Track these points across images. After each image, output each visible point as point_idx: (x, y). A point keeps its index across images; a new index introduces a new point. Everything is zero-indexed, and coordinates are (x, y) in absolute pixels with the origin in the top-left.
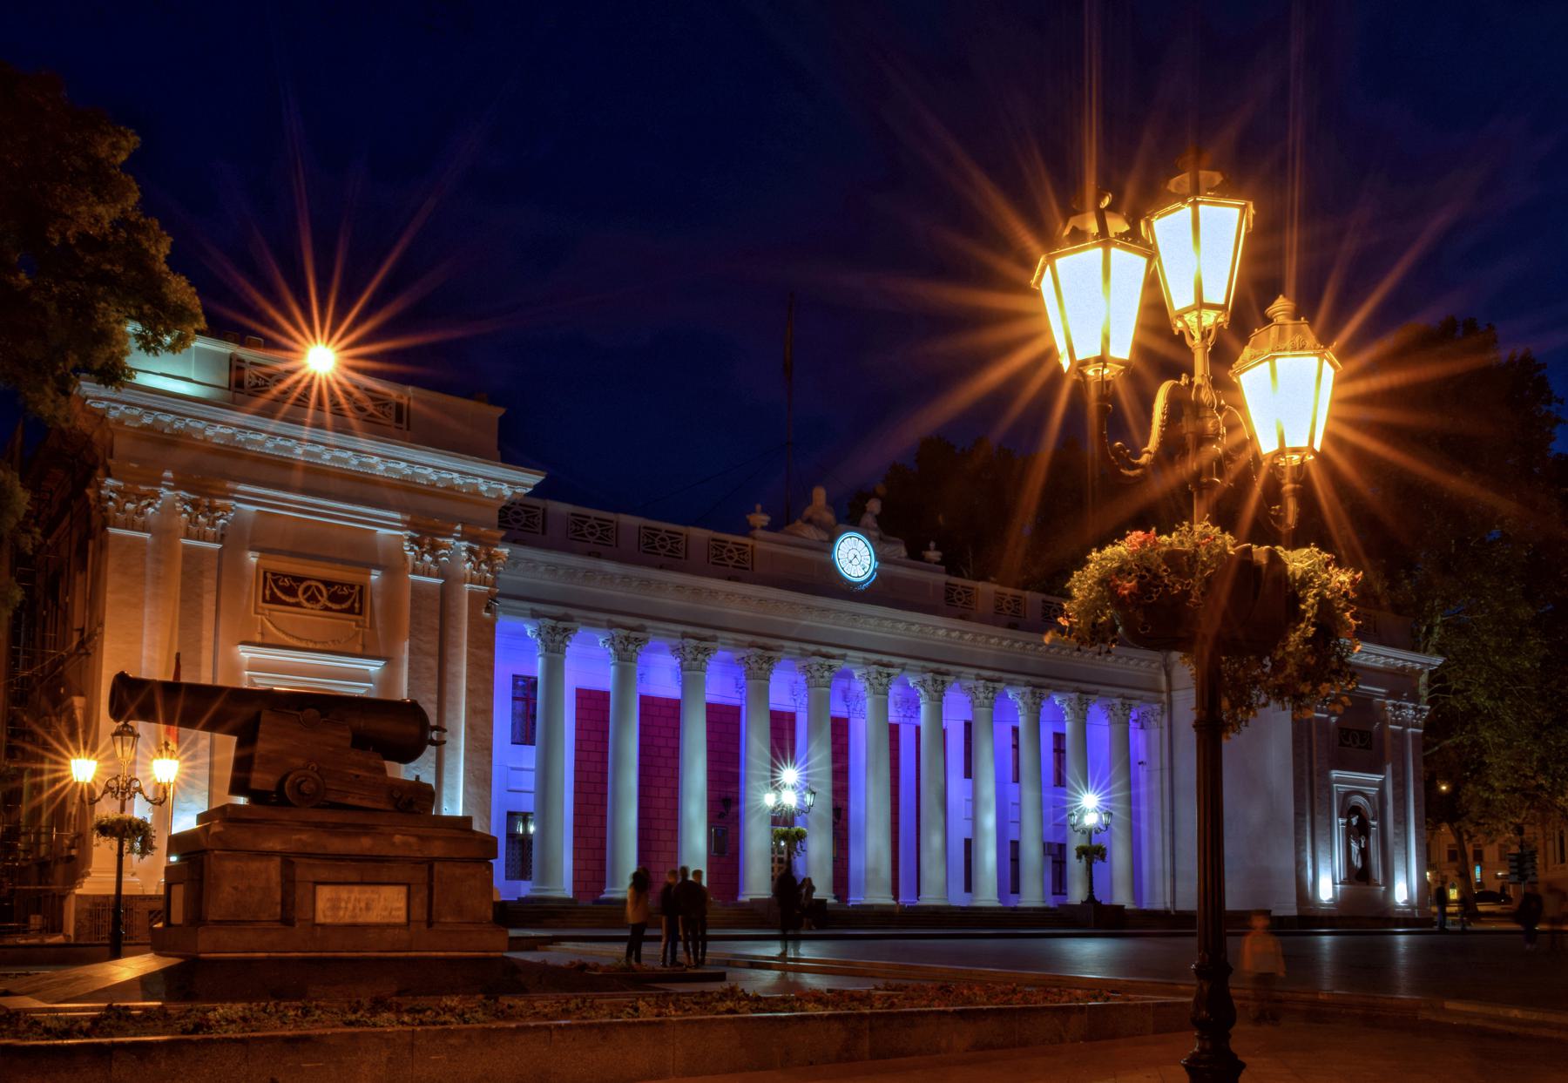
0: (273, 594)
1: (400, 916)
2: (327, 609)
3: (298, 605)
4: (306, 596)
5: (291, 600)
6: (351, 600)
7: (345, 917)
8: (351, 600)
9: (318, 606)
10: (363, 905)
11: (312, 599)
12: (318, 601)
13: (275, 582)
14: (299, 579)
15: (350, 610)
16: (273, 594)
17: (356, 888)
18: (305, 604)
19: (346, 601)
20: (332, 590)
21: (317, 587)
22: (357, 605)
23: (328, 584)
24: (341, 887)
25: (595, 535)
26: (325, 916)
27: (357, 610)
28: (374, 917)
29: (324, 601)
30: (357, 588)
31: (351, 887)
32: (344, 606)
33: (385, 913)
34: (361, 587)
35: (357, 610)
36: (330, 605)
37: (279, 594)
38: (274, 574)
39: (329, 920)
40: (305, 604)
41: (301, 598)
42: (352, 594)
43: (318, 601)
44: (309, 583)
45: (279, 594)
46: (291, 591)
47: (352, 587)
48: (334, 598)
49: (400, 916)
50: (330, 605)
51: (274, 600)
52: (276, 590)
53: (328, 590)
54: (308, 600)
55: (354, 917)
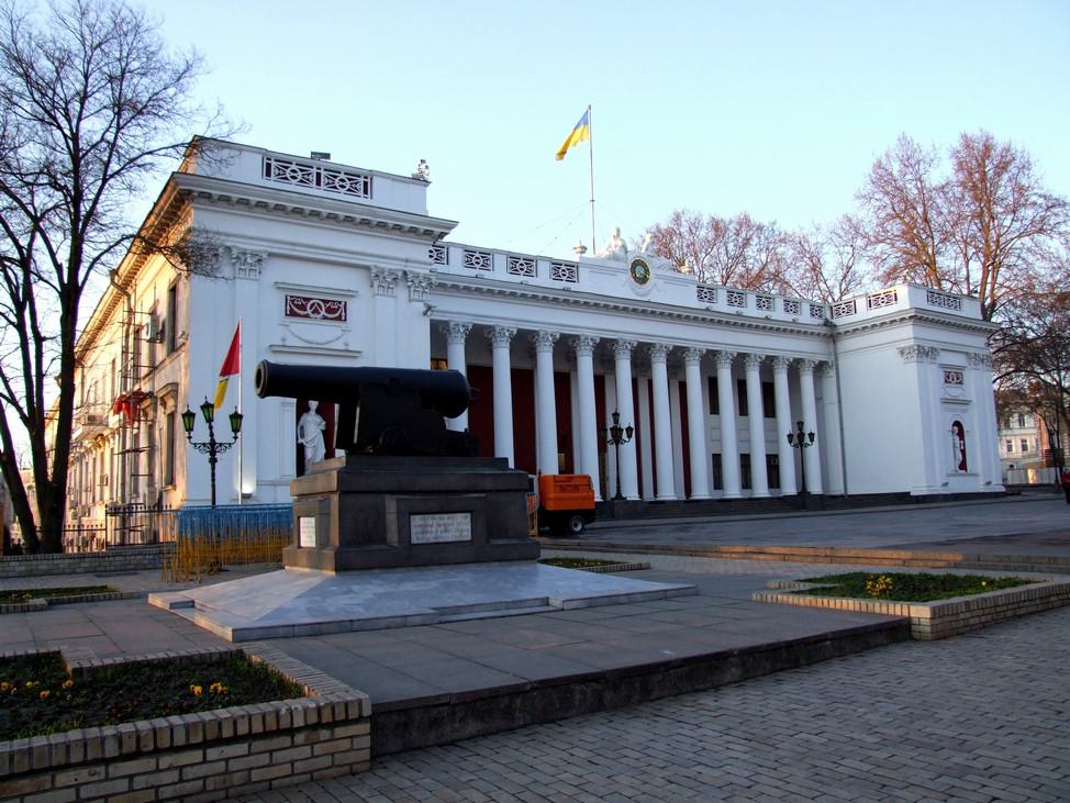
0: (291, 310)
1: (467, 536)
2: (325, 318)
3: (307, 316)
5: (302, 312)
7: (431, 538)
10: (443, 528)
11: (316, 311)
13: (293, 302)
14: (308, 300)
16: (291, 310)
17: (437, 516)
18: (312, 315)
23: (325, 301)
24: (427, 516)
26: (418, 539)
28: (450, 537)
29: (323, 313)
32: (337, 315)
33: (457, 534)
39: (420, 542)
40: (312, 315)
41: (309, 311)
44: (312, 302)
46: (303, 308)
47: (340, 303)
48: (329, 310)
49: (467, 536)
51: (293, 314)
55: (435, 538)
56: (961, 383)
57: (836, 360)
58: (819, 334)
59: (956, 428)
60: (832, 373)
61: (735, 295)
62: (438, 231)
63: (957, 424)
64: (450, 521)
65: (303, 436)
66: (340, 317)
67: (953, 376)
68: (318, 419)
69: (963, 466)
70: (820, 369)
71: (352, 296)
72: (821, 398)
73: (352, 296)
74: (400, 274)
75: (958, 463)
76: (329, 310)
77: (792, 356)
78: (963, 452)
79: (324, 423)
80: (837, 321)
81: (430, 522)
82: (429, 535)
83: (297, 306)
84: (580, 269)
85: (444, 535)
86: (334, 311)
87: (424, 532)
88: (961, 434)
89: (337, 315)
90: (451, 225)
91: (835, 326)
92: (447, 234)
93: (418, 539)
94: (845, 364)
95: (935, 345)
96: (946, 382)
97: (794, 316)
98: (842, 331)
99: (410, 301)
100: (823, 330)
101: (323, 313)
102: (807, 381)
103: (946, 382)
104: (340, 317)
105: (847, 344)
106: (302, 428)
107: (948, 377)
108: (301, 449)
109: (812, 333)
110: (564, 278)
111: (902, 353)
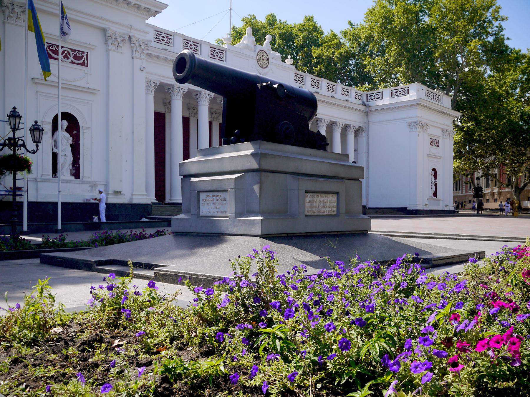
2: (73, 62)
4: (63, 55)
6: (83, 59)
8: (83, 59)
9: (69, 60)
11: (66, 57)
12: (68, 59)
13: (49, 47)
15: (83, 64)
19: (81, 59)
20: (75, 53)
21: (68, 51)
22: (86, 61)
25: (164, 41)
27: (86, 64)
29: (71, 58)
30: (86, 54)
31: (317, 194)
32: (81, 61)
34: (88, 53)
35: (86, 64)
36: (74, 61)
37: (51, 53)
38: (48, 43)
42: (83, 56)
43: (68, 59)
45: (51, 53)
47: (84, 52)
50: (74, 61)
52: (49, 51)
53: (73, 53)
54: (64, 57)
55: (318, 212)
56: (437, 146)
57: (367, 127)
58: (360, 110)
59: (433, 172)
60: (364, 134)
61: (315, 81)
62: (154, 9)
63: (434, 170)
64: (326, 199)
65: (56, 148)
66: (84, 63)
67: (434, 143)
68: (67, 135)
69: (435, 194)
70: (357, 132)
71: (93, 49)
72: (355, 150)
73: (93, 49)
74: (127, 38)
75: (433, 192)
76: (75, 57)
77: (344, 122)
78: (436, 185)
79: (71, 139)
80: (370, 103)
81: (315, 199)
82: (314, 209)
83: (52, 51)
84: (228, 53)
85: (323, 209)
86: (79, 58)
87: (312, 207)
88: (435, 176)
89: (81, 61)
90: (165, 6)
91: (369, 106)
92: (159, 12)
93: (308, 212)
94: (373, 129)
95: (427, 122)
96: (431, 145)
97: (347, 98)
98: (373, 110)
99: (133, 58)
100: (362, 108)
101: (71, 58)
102: (351, 137)
103: (431, 145)
104: (84, 63)
105: (374, 118)
106: (55, 141)
107: (432, 142)
108: (55, 156)
109: (356, 109)
110: (217, 58)
111: (410, 125)
